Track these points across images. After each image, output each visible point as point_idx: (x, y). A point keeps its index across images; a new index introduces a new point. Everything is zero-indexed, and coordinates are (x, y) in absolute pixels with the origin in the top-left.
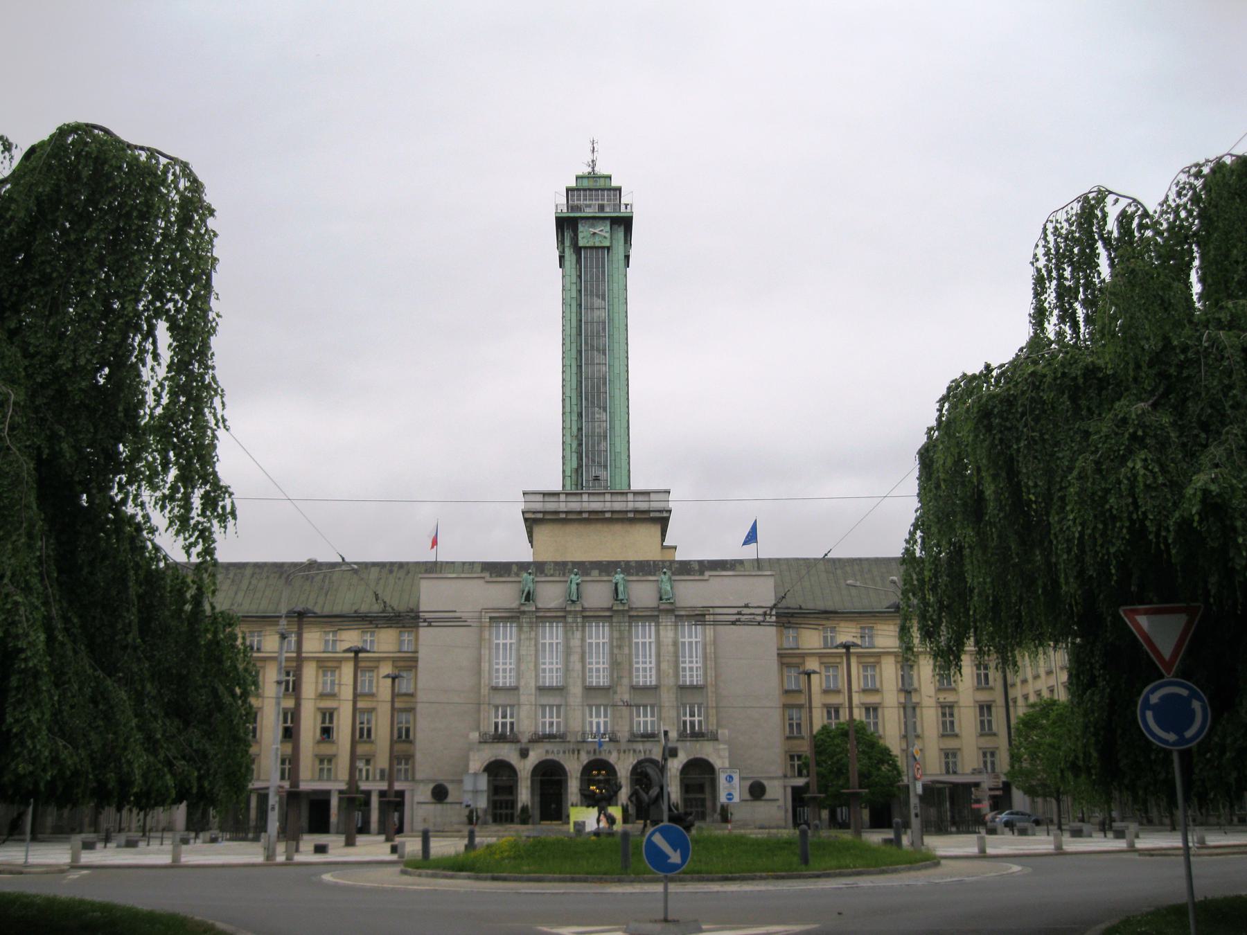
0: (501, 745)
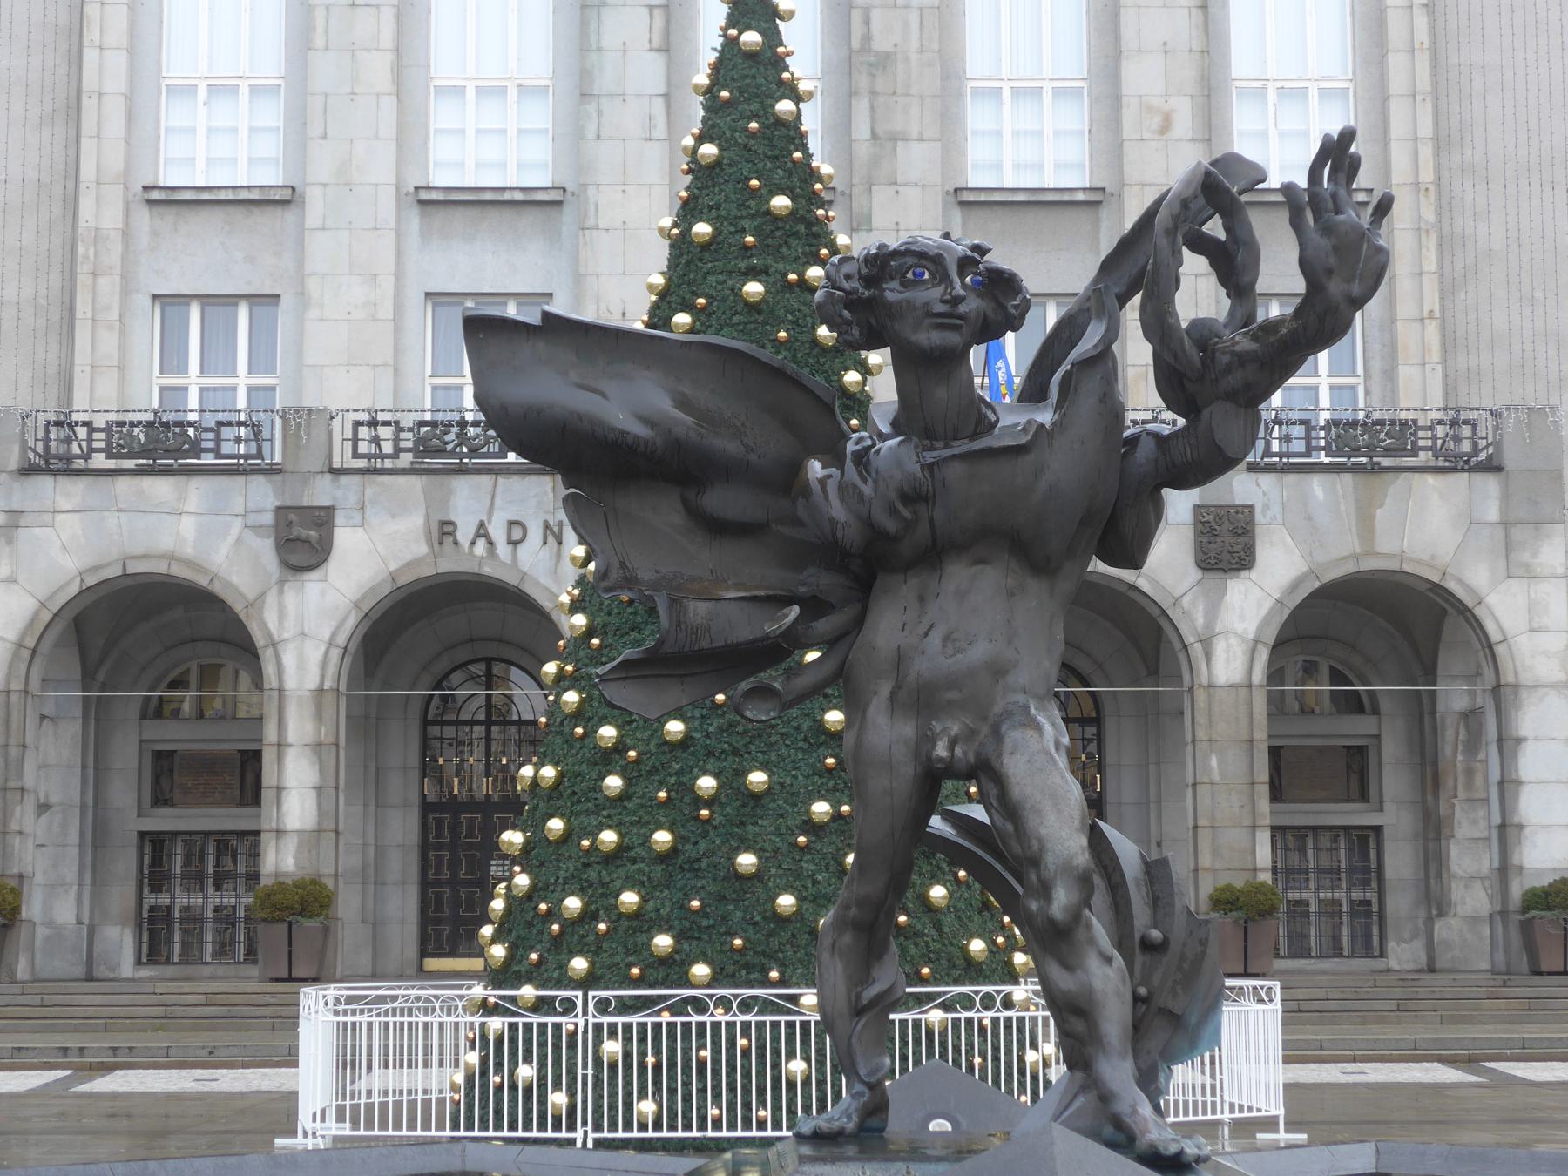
0: (161, 488)
